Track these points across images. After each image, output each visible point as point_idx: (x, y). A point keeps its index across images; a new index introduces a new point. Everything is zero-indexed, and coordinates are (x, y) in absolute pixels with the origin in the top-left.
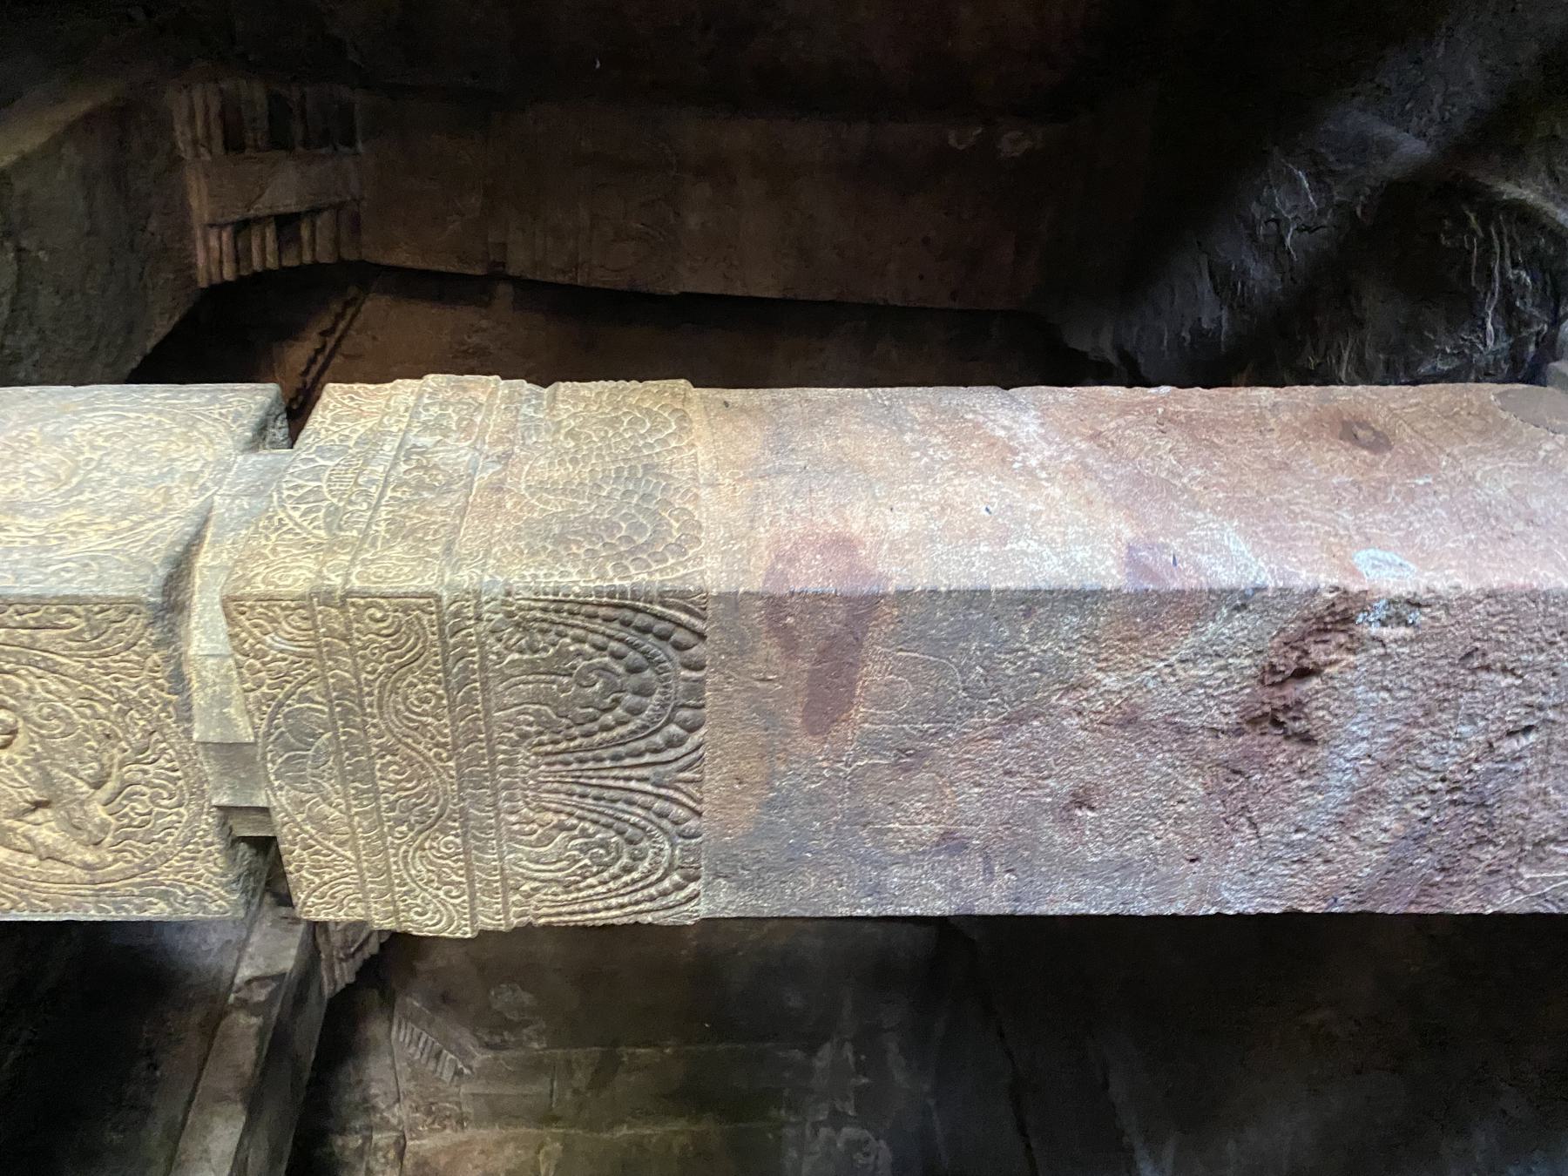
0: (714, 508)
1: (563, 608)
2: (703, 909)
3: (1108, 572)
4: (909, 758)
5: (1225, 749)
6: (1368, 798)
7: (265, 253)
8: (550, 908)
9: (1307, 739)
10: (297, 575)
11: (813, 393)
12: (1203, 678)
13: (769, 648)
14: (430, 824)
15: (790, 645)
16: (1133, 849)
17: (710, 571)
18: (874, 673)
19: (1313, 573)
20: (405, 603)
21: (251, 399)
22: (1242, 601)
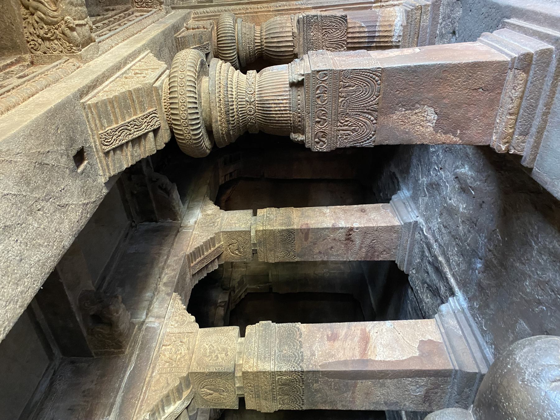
0: (296, 221)
1: (283, 230)
2: (296, 260)
3: (330, 226)
4: (315, 244)
5: (345, 242)
6: (361, 248)
7: (228, 179)
8: (281, 260)
9: (352, 241)
10: (261, 228)
11: (307, 208)
12: (341, 235)
13: (301, 233)
14: (271, 251)
15: (302, 233)
16: (338, 253)
17: (295, 227)
18: (310, 236)
19: (349, 225)
20: (270, 230)
21: (251, 211)
22: (342, 228)
